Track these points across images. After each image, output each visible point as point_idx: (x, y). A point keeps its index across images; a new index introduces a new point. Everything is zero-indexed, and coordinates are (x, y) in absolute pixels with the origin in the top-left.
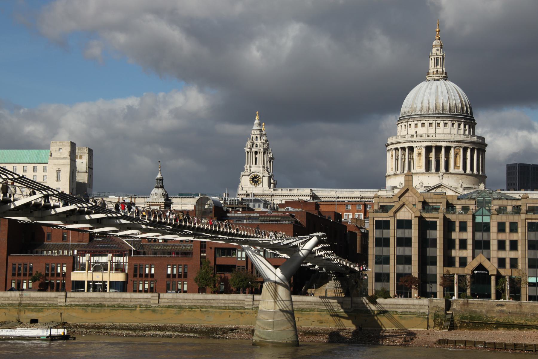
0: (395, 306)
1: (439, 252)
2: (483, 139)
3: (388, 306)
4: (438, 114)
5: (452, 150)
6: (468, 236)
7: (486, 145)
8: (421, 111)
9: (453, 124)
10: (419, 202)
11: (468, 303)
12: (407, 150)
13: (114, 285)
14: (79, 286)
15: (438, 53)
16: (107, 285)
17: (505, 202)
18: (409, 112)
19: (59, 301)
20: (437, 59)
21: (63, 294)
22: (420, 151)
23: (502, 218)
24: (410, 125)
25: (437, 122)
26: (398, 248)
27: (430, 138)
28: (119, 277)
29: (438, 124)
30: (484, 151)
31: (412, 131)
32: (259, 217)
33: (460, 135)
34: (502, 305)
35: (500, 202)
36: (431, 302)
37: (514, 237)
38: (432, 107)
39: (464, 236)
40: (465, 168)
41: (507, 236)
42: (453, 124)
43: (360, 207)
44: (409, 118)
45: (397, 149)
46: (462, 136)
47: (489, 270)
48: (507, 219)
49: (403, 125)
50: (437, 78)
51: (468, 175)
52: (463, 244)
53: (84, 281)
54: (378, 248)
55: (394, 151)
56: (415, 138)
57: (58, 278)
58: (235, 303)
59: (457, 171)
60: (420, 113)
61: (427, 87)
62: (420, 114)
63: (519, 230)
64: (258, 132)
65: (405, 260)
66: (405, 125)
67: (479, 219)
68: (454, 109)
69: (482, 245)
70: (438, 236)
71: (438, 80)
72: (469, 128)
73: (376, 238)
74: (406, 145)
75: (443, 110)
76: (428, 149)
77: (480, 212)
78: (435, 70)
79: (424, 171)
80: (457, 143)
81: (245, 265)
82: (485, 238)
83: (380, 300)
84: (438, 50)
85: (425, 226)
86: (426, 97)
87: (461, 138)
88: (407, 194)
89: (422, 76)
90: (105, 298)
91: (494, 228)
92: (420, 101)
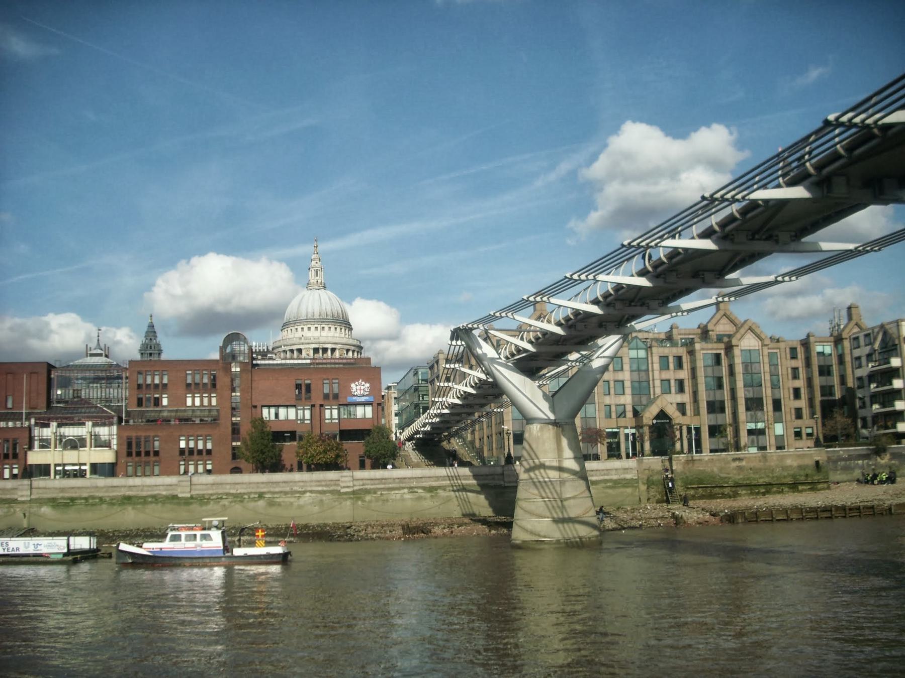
6: (626, 376)
11: (693, 460)
12: (295, 352)
19: (20, 493)
20: (317, 271)
28: (106, 456)
32: (310, 364)
34: (740, 459)
36: (640, 462)
39: (620, 376)
41: (672, 375)
53: (49, 465)
56: (303, 341)
57: (7, 461)
68: (336, 315)
76: (316, 350)
87: (344, 341)
90: (97, 487)
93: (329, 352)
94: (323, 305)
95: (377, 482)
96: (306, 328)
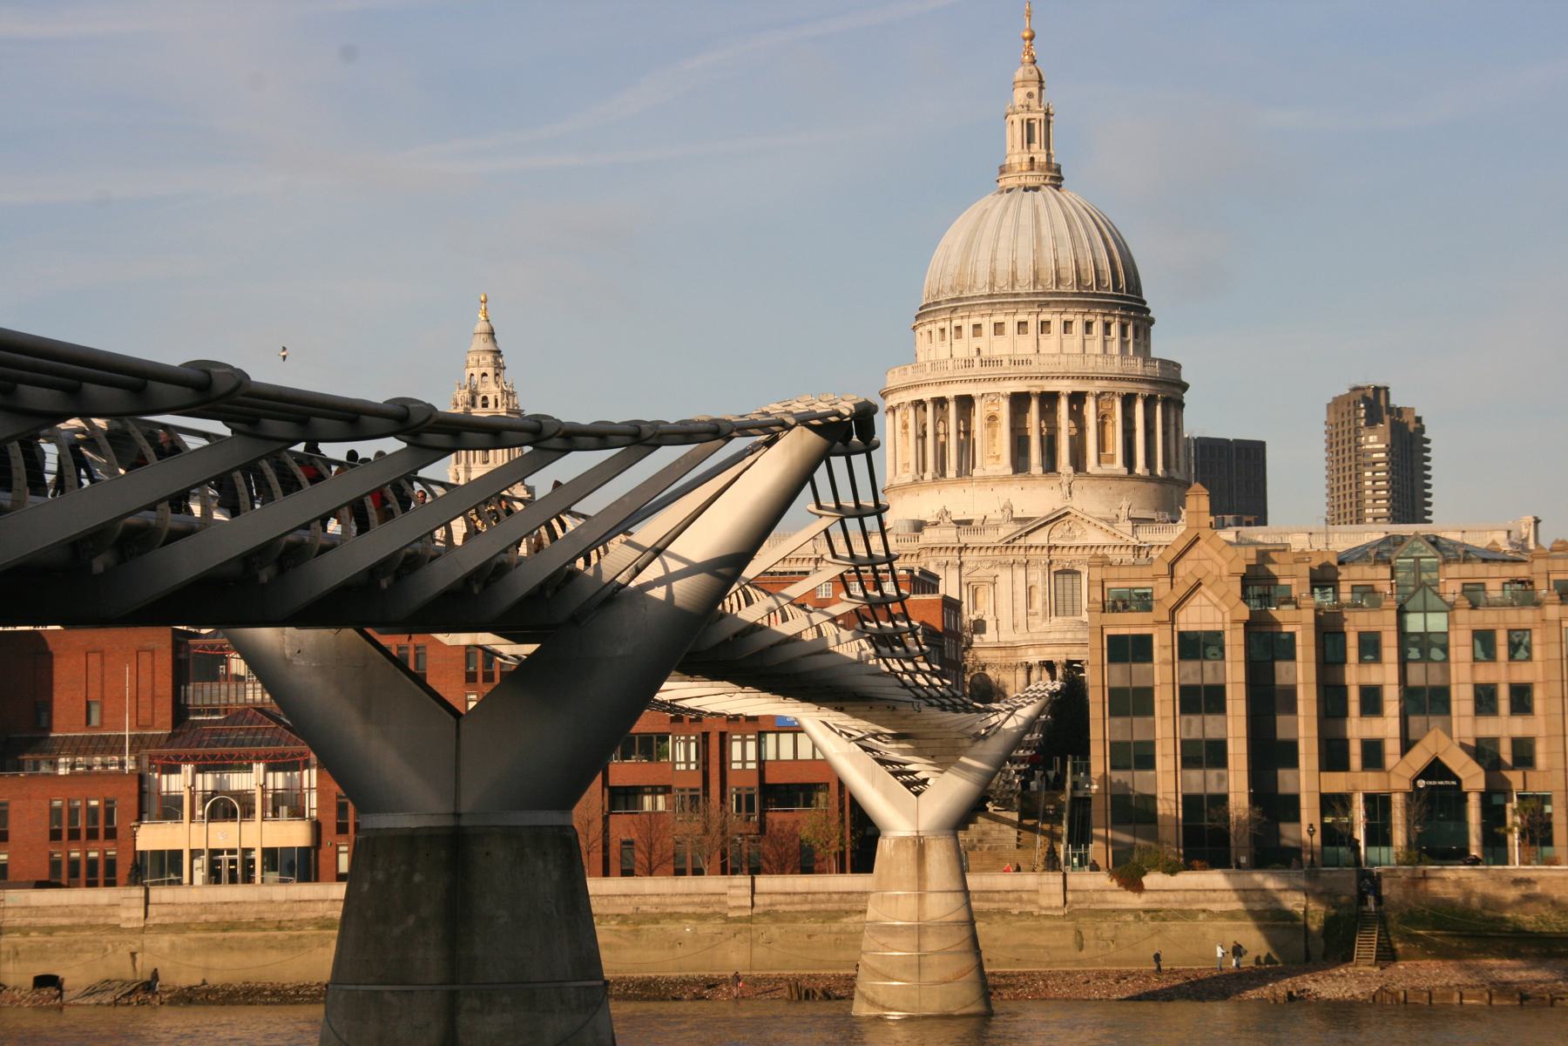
0: (1201, 896)
1: (1304, 727)
2: (1179, 366)
3: (1180, 896)
4: (1044, 294)
5: (1090, 409)
6: (1386, 675)
7: (1185, 387)
8: (992, 285)
9: (1088, 325)
10: (1232, 574)
14: (168, 865)
15: (1034, 102)
16: (252, 861)
17: (1477, 571)
18: (952, 289)
19: (124, 914)
20: (1030, 127)
21: (138, 892)
22: (993, 409)
23: (1485, 618)
24: (959, 328)
25: (1043, 317)
26: (1185, 718)
27: (1024, 369)
29: (1045, 326)
30: (1180, 405)
31: (964, 347)
33: (1112, 357)
34: (1528, 881)
35: (1466, 570)
37: (1522, 673)
38: (1025, 274)
39: (1373, 675)
40: (1129, 460)
41: (1501, 674)
42: (1088, 325)
44: (956, 309)
45: (919, 404)
46: (1117, 360)
47: (1460, 775)
48: (1501, 621)
49: (935, 328)
50: (1031, 182)
51: (1140, 478)
52: (1372, 701)
53: (180, 852)
54: (1118, 721)
55: (911, 411)
56: (977, 369)
57: (93, 844)
58: (694, 904)
59: (1106, 469)
60: (987, 291)
61: (1006, 209)
62: (990, 296)
63: (1537, 652)
64: (489, 358)
65: (1209, 754)
66: (943, 330)
67: (1415, 623)
68: (1091, 278)
69: (1426, 702)
70: (1300, 679)
71: (1036, 189)
72: (1136, 336)
73: (1110, 690)
74: (950, 392)
75: (1059, 281)
76: (1019, 402)
77: (1417, 601)
78: (1026, 158)
79: (1009, 471)
80: (1105, 383)
81: (698, 784)
82: (1436, 679)
83: (1152, 880)
84: (1030, 95)
85: (1266, 646)
86: (1003, 243)
87: (1115, 367)
88: (1193, 553)
91: (1461, 648)
92: (984, 255)
93: (1063, 407)
94: (1048, 242)
95: (797, 898)
96: (987, 328)
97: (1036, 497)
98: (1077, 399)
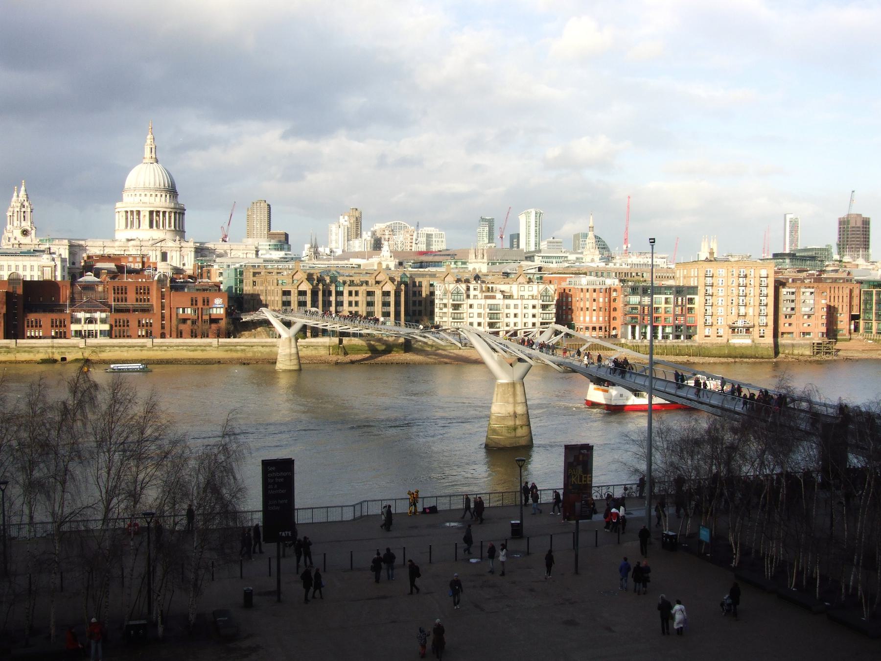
5: (167, 214)
13: (102, 332)
23: (351, 288)
28: (106, 327)
30: (183, 214)
31: (138, 199)
37: (357, 299)
41: (353, 299)
43: (139, 259)
45: (127, 212)
55: (124, 214)
69: (339, 304)
74: (135, 209)
76: (151, 213)
89: (140, 160)
91: (346, 293)
96: (143, 194)
97: (157, 234)
98: (164, 212)
